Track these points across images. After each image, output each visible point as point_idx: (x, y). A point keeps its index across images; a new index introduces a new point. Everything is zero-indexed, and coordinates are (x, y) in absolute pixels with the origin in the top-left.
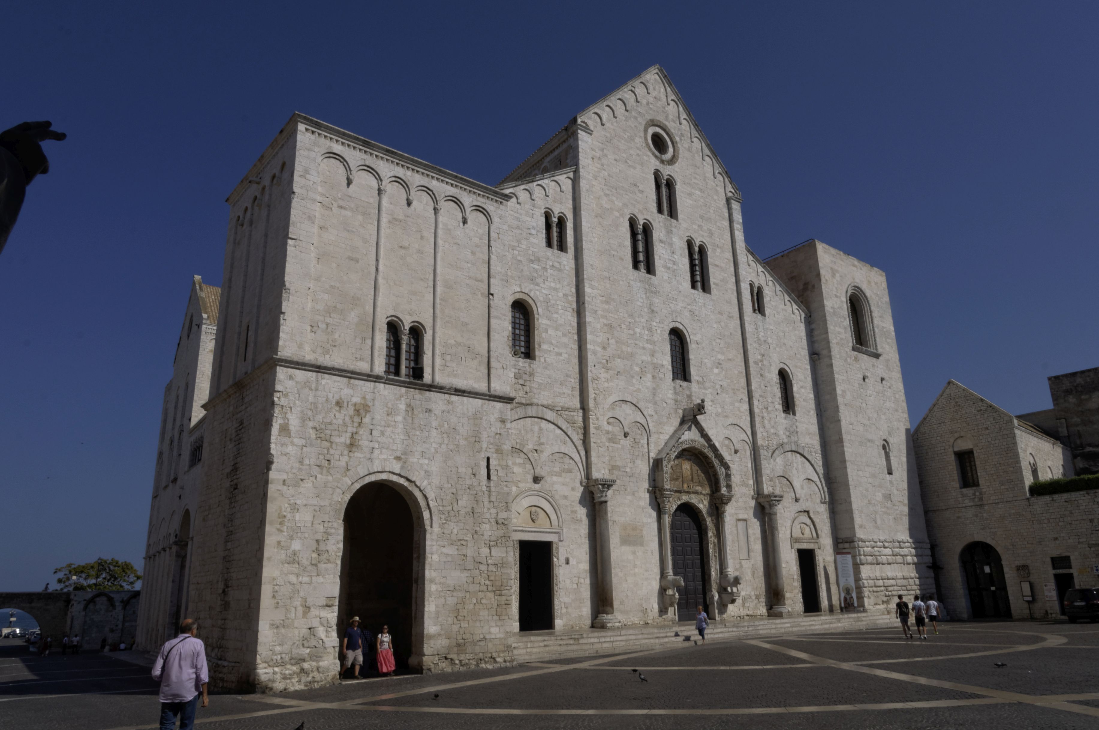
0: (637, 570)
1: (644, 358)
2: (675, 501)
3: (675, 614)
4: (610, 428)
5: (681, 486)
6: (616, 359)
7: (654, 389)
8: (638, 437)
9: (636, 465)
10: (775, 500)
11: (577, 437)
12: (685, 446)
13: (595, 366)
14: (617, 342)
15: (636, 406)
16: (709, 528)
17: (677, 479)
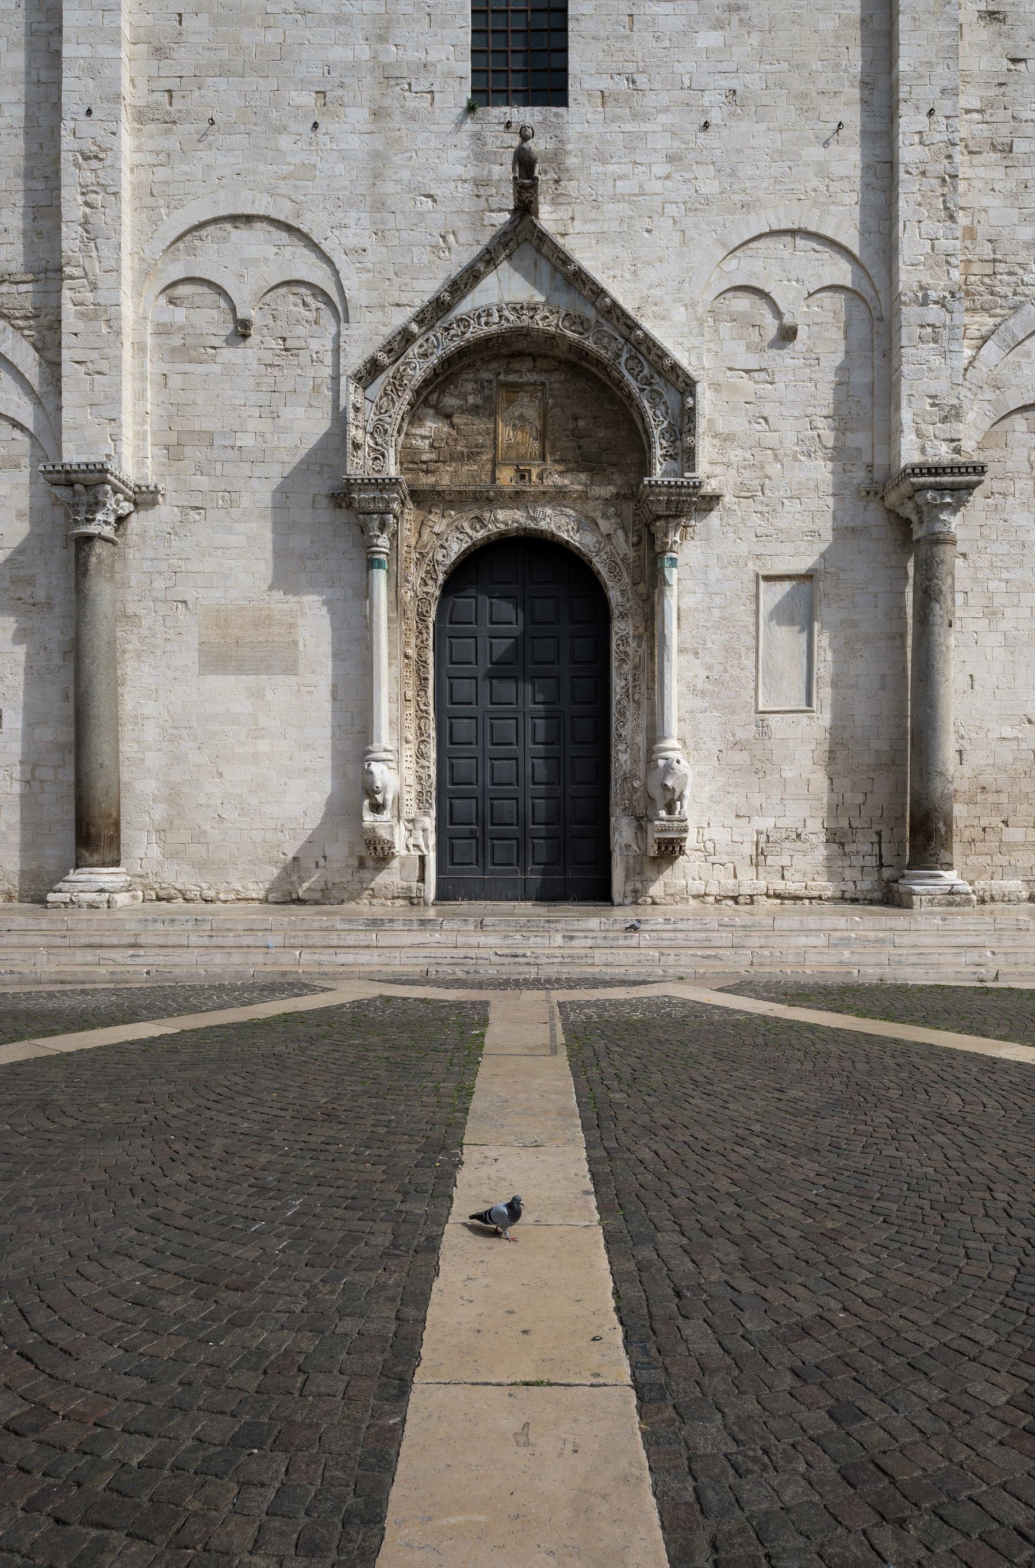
0: (263, 745)
1: (337, 54)
2: (460, 530)
3: (422, 879)
4: (179, 315)
5: (485, 477)
6: (210, 81)
7: (376, 155)
8: (301, 331)
9: (281, 422)
10: (939, 488)
11: (27, 360)
12: (476, 331)
13: (89, 112)
14: (216, 21)
15: (289, 229)
16: (616, 612)
17: (472, 456)
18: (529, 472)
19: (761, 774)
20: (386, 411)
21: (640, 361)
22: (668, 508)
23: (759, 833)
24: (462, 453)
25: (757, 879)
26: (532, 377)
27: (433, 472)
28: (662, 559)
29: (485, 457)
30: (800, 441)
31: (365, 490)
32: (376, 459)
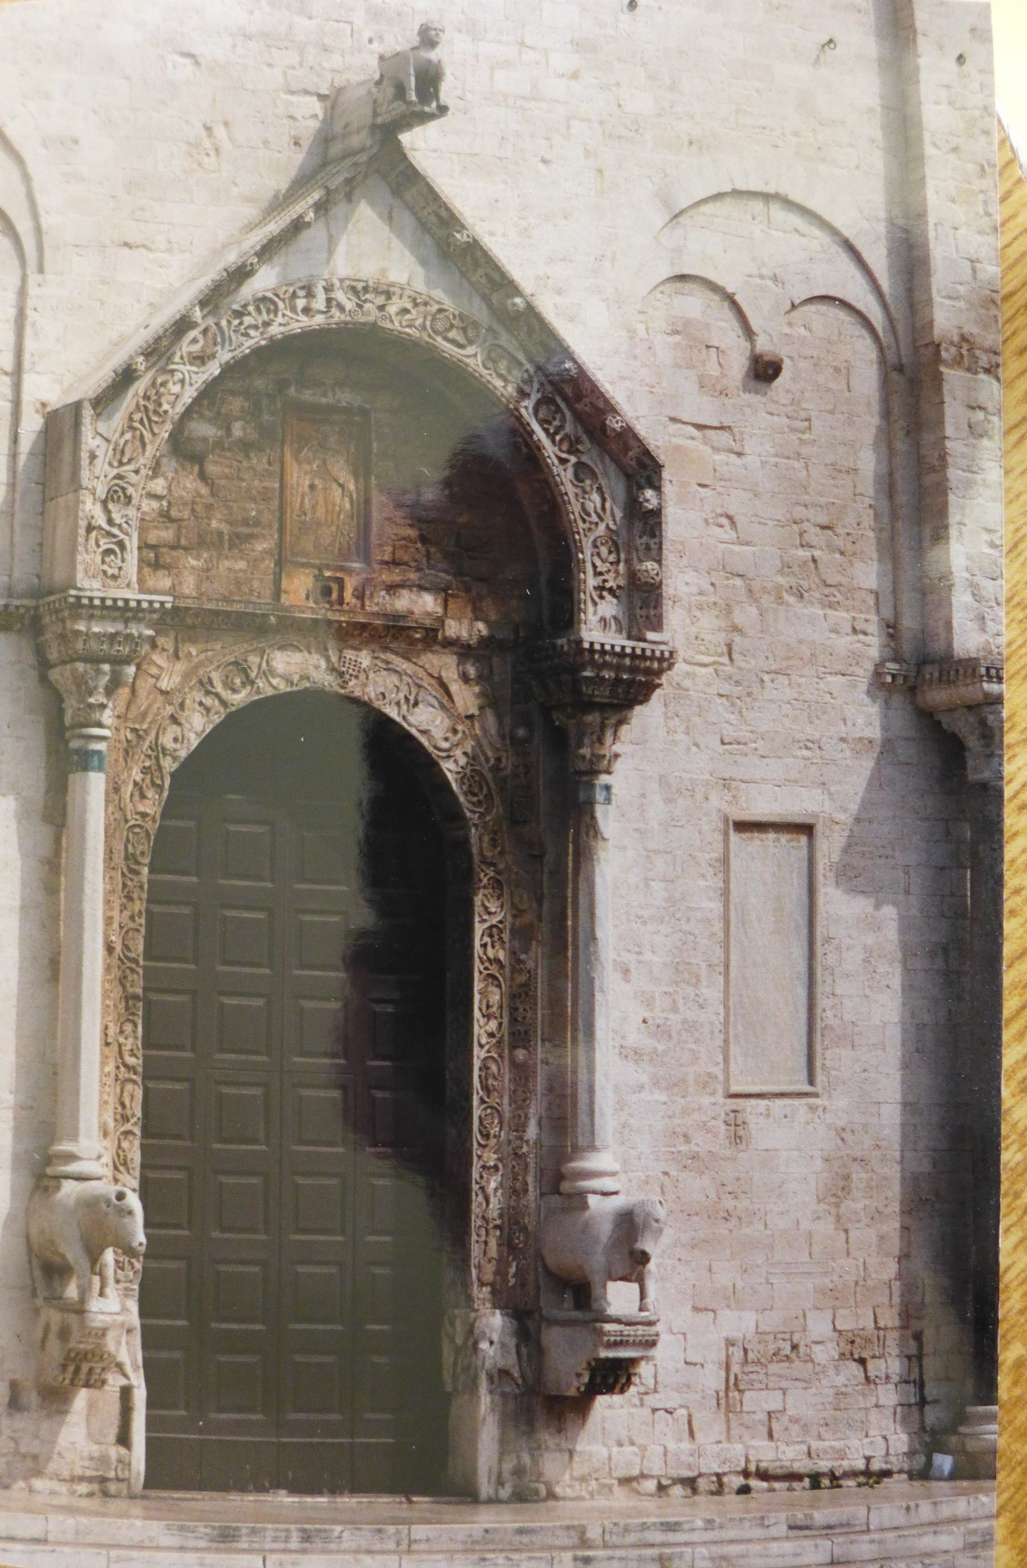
17: (238, 541)
18: (340, 582)
19: (734, 1221)
20: (130, 461)
21: (558, 410)
22: (613, 693)
23: (730, 1343)
24: (220, 534)
25: (729, 1438)
26: (346, 397)
27: (168, 567)
28: (591, 786)
29: (260, 546)
30: (786, 567)
31: (102, 618)
32: (108, 552)
